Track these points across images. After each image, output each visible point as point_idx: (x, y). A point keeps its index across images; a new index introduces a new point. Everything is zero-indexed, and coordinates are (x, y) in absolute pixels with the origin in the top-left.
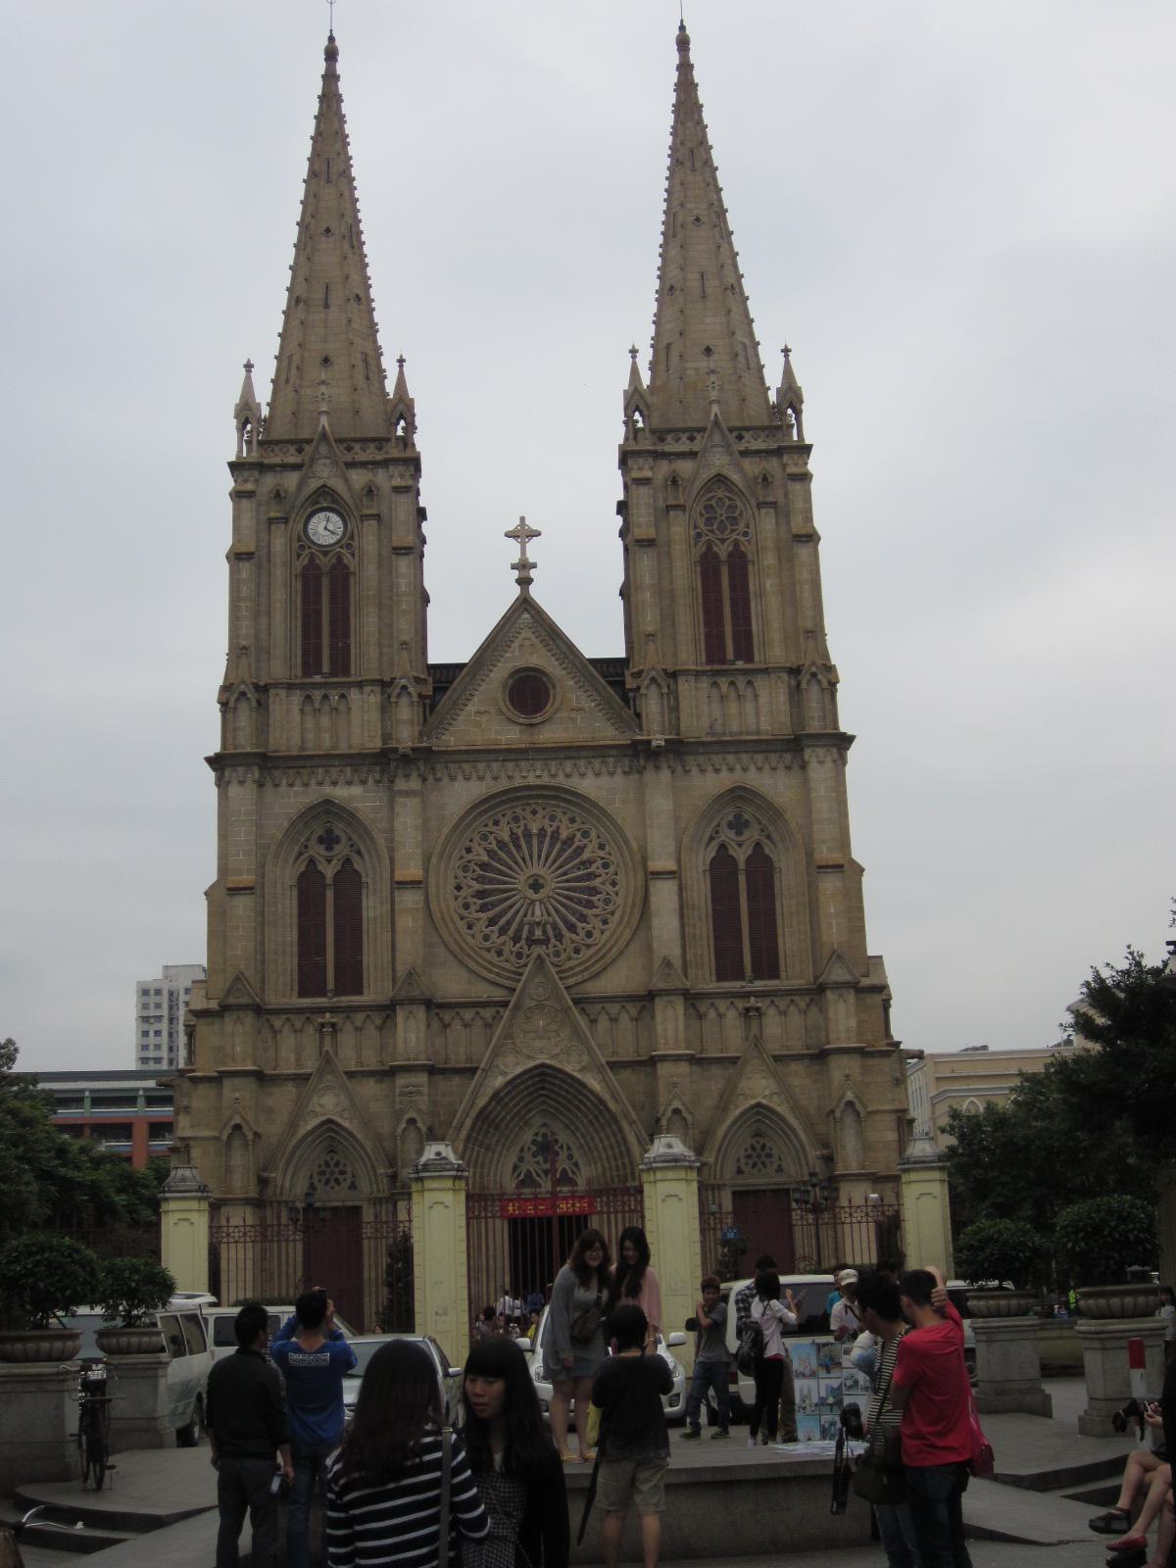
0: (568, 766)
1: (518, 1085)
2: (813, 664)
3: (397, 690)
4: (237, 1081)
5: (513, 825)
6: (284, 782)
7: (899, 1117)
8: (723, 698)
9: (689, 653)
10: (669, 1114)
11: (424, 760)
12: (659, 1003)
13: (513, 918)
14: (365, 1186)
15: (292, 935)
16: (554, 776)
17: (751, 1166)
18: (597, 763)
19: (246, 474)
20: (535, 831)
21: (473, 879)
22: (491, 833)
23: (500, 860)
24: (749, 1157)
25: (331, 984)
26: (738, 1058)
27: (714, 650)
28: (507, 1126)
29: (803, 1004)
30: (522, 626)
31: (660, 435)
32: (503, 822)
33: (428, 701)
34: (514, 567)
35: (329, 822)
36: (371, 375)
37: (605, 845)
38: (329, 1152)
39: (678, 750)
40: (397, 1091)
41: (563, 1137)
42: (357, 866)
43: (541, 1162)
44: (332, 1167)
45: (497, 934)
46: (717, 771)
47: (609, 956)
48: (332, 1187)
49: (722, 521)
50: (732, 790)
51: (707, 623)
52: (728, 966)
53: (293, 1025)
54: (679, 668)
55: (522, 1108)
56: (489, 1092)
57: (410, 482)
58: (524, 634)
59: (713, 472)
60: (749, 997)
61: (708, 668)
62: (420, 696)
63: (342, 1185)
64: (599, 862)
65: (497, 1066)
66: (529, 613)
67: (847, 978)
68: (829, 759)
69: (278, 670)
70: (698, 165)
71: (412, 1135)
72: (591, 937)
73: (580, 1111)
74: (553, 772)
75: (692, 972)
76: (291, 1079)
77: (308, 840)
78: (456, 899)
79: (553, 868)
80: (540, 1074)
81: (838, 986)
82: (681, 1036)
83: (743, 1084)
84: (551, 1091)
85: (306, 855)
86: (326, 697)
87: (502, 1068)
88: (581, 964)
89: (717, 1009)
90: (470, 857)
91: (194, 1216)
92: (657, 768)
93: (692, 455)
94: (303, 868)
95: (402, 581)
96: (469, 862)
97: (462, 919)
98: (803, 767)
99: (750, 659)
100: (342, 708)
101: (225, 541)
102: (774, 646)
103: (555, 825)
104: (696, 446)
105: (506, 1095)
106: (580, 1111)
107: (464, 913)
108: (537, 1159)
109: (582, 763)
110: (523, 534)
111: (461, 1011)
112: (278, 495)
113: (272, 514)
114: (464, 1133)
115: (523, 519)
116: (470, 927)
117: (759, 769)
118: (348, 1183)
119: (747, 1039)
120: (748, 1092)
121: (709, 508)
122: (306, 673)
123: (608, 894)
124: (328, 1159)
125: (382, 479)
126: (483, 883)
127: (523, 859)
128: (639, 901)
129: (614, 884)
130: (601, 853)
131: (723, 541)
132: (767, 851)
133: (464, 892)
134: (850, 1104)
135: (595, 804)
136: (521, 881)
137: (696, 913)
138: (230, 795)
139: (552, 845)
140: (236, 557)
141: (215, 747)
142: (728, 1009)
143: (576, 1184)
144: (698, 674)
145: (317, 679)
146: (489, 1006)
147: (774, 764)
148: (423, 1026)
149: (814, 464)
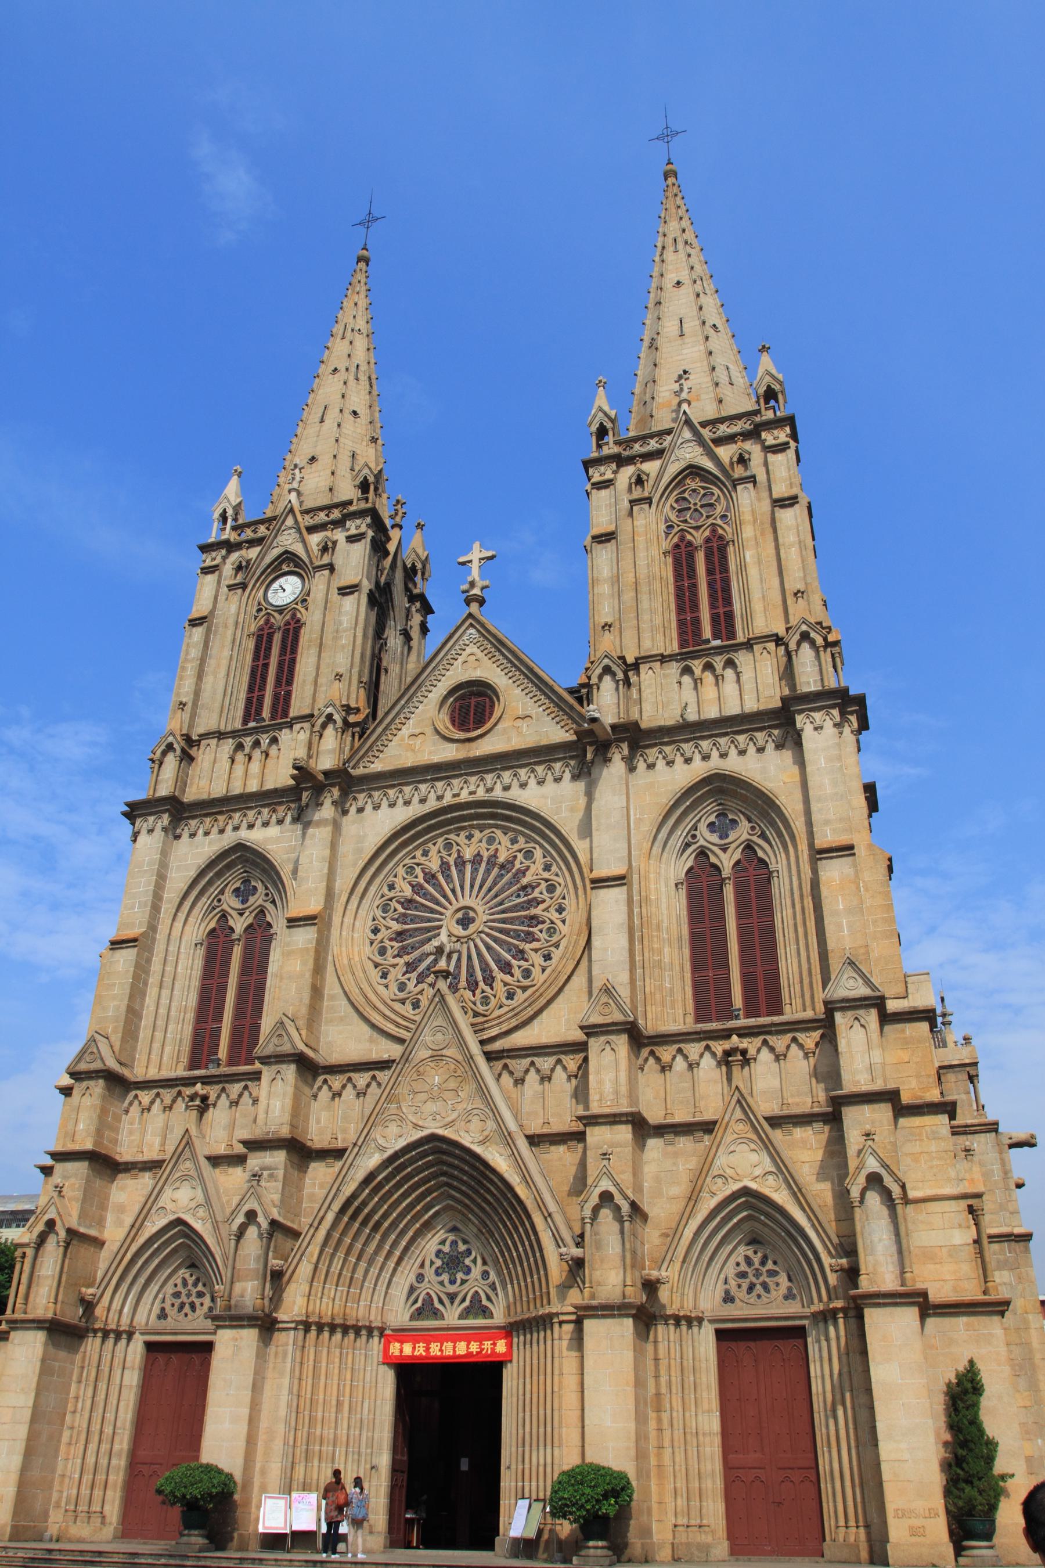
0: (507, 776)
2: (804, 622)
3: (322, 719)
5: (444, 853)
6: (201, 832)
7: (970, 1207)
8: (697, 682)
16: (489, 790)
17: (745, 1286)
18: (540, 769)
21: (393, 920)
22: (418, 865)
23: (426, 895)
24: (743, 1275)
25: (223, 1052)
26: (715, 1123)
28: (394, 1224)
29: (812, 1045)
30: (467, 642)
31: (628, 442)
32: (433, 850)
33: (357, 729)
35: (245, 872)
37: (550, 866)
43: (446, 1282)
44: (190, 1287)
46: (688, 761)
48: (186, 1315)
49: (696, 510)
51: (680, 609)
56: (360, 1175)
57: (363, 528)
58: (469, 650)
60: (729, 1037)
62: (345, 722)
64: (544, 885)
65: (375, 1140)
66: (475, 628)
68: (828, 724)
72: (528, 977)
76: (150, 1169)
77: (222, 892)
78: (372, 943)
83: (722, 1160)
84: (452, 1177)
86: (257, 744)
92: (607, 760)
94: (212, 925)
97: (376, 967)
100: (273, 751)
103: (493, 848)
105: (387, 1179)
107: (378, 959)
108: (440, 1279)
109: (523, 772)
111: (355, 1076)
113: (232, 582)
116: (384, 976)
117: (742, 753)
120: (729, 1172)
123: (552, 922)
125: (339, 535)
126: (405, 923)
127: (453, 891)
129: (560, 910)
130: (546, 875)
131: (697, 528)
132: (760, 854)
133: (380, 936)
134: (874, 1180)
139: (488, 872)
142: (701, 1056)
143: (491, 1316)
144: (663, 659)
147: (761, 743)
148: (290, 1090)
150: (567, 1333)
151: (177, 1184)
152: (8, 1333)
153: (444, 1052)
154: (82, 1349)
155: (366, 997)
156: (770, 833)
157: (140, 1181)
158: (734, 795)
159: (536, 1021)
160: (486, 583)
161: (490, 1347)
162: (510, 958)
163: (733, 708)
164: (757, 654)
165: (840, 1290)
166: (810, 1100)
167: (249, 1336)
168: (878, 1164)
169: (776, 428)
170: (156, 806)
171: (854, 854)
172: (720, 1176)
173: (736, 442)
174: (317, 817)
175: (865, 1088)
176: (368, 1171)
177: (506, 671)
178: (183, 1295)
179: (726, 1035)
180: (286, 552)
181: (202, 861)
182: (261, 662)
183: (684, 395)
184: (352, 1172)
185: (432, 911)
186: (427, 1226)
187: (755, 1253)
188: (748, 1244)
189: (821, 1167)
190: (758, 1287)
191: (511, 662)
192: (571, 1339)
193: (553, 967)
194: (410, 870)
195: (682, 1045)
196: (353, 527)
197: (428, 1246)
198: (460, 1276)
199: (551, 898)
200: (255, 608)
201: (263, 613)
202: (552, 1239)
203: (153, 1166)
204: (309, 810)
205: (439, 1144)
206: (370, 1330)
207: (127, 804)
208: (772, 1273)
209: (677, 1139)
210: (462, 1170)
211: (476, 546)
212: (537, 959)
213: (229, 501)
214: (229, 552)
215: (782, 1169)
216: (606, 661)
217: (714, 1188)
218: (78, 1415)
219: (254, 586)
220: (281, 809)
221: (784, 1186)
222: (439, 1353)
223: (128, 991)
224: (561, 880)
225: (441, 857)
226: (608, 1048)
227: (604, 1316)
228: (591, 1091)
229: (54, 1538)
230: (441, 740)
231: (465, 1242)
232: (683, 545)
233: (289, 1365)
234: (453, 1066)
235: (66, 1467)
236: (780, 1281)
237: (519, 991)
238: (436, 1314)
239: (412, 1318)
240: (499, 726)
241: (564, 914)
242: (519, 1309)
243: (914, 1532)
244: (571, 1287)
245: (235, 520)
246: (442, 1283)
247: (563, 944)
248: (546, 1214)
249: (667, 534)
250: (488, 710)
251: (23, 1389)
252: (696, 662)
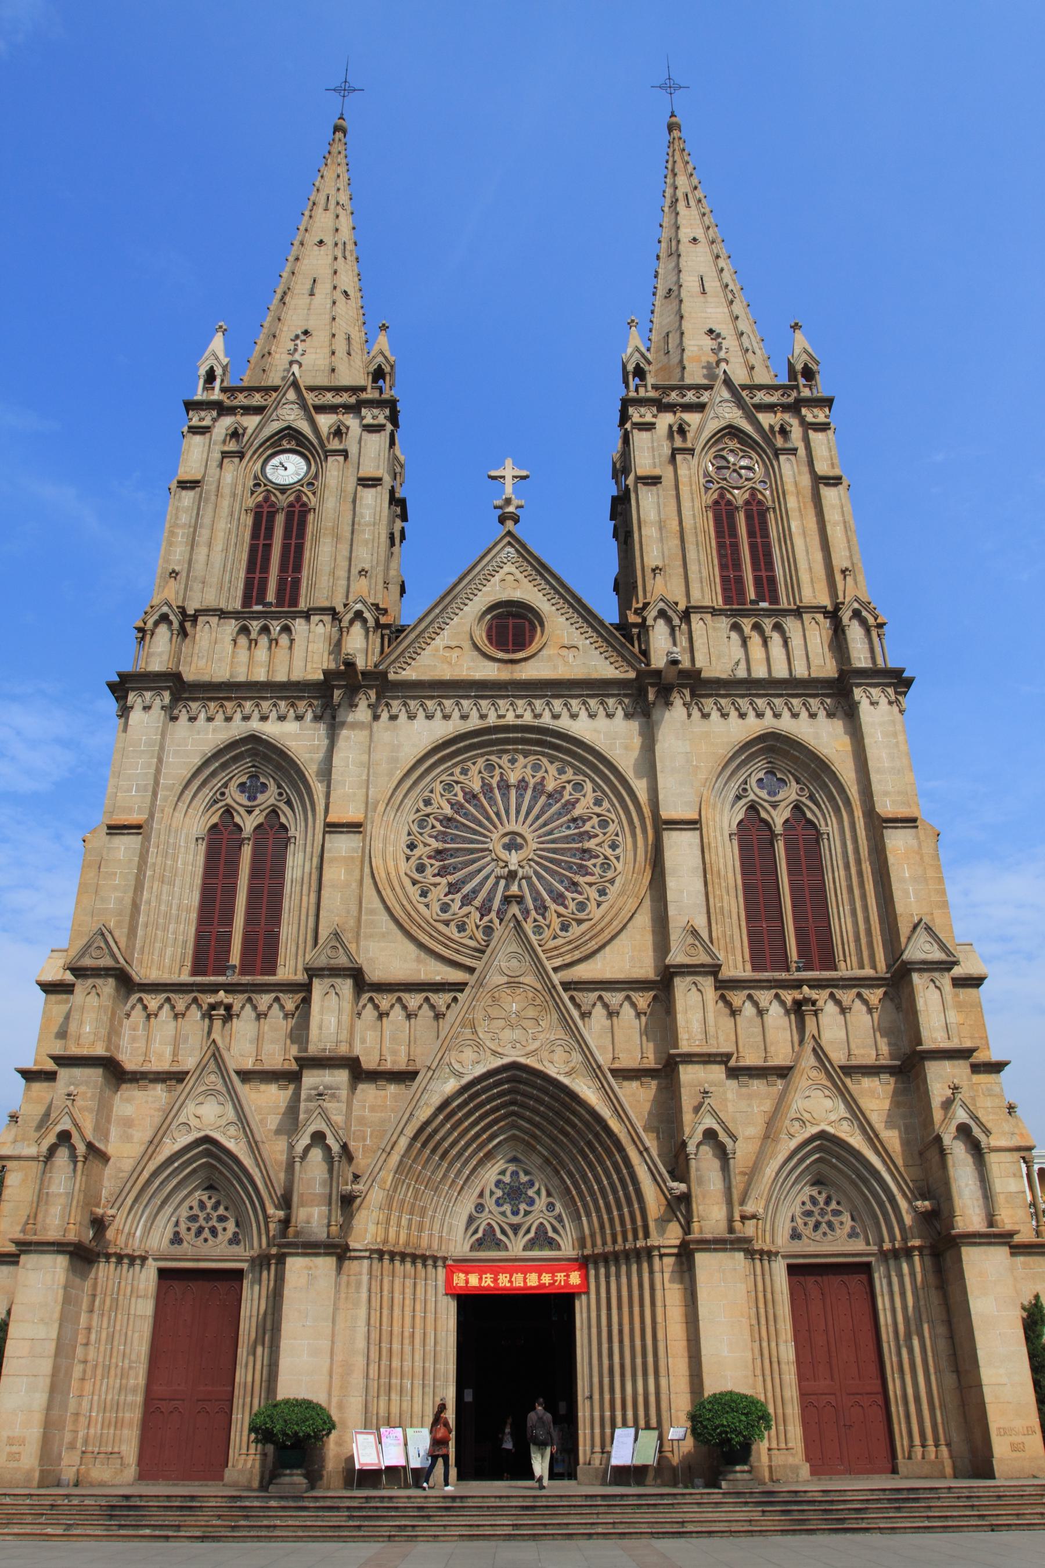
0: (557, 704)
1: (477, 1094)
2: (857, 600)
3: (350, 615)
4: (78, 1072)
5: (486, 775)
6: (202, 716)
10: (698, 1136)
12: (680, 984)
13: (482, 884)
15: (193, 899)
16: (537, 716)
17: (811, 1224)
18: (593, 702)
19: (203, 414)
21: (431, 836)
22: (457, 783)
23: (466, 815)
24: (808, 1214)
25: (235, 958)
26: (790, 1068)
27: (732, 587)
28: (460, 1154)
29: (876, 1002)
30: (505, 560)
32: (474, 770)
33: (387, 632)
35: (253, 766)
36: (352, 352)
37: (602, 800)
38: (206, 1189)
40: (303, 1096)
42: (286, 817)
43: (509, 1213)
44: (209, 1210)
45: (460, 904)
47: (606, 932)
48: (206, 1240)
51: (723, 567)
53: (173, 1007)
54: (693, 603)
55: (484, 1130)
56: (436, 1100)
57: (381, 420)
58: (507, 568)
59: (723, 423)
60: (800, 987)
61: (728, 607)
62: (377, 621)
63: (220, 1236)
64: (595, 820)
65: (450, 1065)
66: (513, 546)
67: (938, 955)
68: (883, 701)
69: (211, 599)
70: (692, 203)
71: (316, 1155)
72: (584, 910)
73: (566, 1134)
74: (538, 711)
76: (163, 1081)
77: (226, 785)
78: (408, 859)
79: (535, 826)
80: (508, 1080)
85: (223, 803)
86: (265, 630)
87: (457, 1066)
88: (570, 942)
89: (756, 1004)
90: (429, 810)
92: (668, 704)
93: (700, 407)
94: (215, 819)
96: (428, 815)
97: (414, 884)
99: (775, 599)
100: (284, 640)
103: (539, 775)
104: (705, 397)
105: (460, 1107)
106: (566, 1134)
107: (417, 876)
108: (502, 1209)
109: (574, 702)
111: (406, 996)
112: (235, 435)
113: (226, 449)
114: (395, 1158)
116: (424, 894)
117: (795, 715)
118: (229, 1234)
119: (801, 1041)
120: (806, 1116)
122: (247, 600)
123: (606, 858)
124: (205, 1198)
125: (351, 421)
126: (445, 842)
127: (497, 814)
129: (614, 846)
130: (597, 810)
132: (809, 815)
133: (417, 852)
136: (496, 842)
137: (723, 884)
138: (130, 722)
139: (535, 799)
143: (559, 1248)
145: (258, 608)
146: (444, 991)
147: (814, 709)
149: (835, 416)
150: (668, 1266)
151: (201, 1099)
152: (18, 1256)
153: (521, 979)
154: (92, 1275)
155: (409, 915)
157: (151, 1093)
158: (785, 754)
159: (598, 956)
160: (522, 502)
161: (563, 1278)
162: (563, 890)
163: (781, 671)
164: (806, 623)
165: (915, 1230)
166: (874, 1053)
167: (326, 1264)
168: (967, 1116)
169: (816, 407)
170: (154, 681)
171: (917, 827)
172: (797, 1119)
173: (775, 413)
174: (351, 718)
175: (945, 1045)
176: (446, 1096)
177: (549, 597)
178: (201, 1219)
179: (797, 985)
180: (289, 428)
181: (208, 749)
182: (262, 542)
183: (722, 354)
184: (426, 1096)
185: (475, 832)
186: (489, 1156)
187: (820, 1193)
188: (813, 1185)
189: (889, 1116)
190: (824, 1225)
191: (553, 588)
192: (672, 1272)
193: (611, 902)
194: (448, 787)
195: (752, 992)
196: (369, 416)
197: (487, 1176)
198: (523, 1207)
199: (605, 834)
200: (252, 483)
201: (262, 489)
202: (648, 1173)
203: (176, 1077)
204: (341, 709)
205: (518, 1073)
206: (435, 1259)
207: (120, 675)
208: (836, 1213)
209: (751, 1081)
210: (541, 1102)
211: (509, 462)
212: (593, 893)
213: (217, 358)
214: (219, 415)
215: (857, 1114)
216: (662, 605)
217: (792, 1131)
218: (91, 1348)
219: (251, 457)
220: (302, 705)
221: (858, 1131)
222: (508, 1285)
223: (133, 883)
224: (614, 817)
225: (482, 778)
226: (694, 989)
227: (716, 1250)
228: (680, 1030)
229: (71, 1484)
230: (480, 657)
231: (527, 1173)
232: (723, 503)
233: (364, 1295)
234: (531, 995)
235: (80, 1404)
236: (844, 1220)
237: (573, 923)
238: (499, 1245)
239: (472, 1248)
240: (544, 652)
241: (618, 851)
242: (599, 1241)
243: (1015, 1447)
244: (670, 1221)
245: (222, 381)
246: (503, 1214)
247: (618, 880)
248: (642, 1149)
249: (707, 489)
250: (527, 634)
251: (42, 1320)
252: (745, 620)
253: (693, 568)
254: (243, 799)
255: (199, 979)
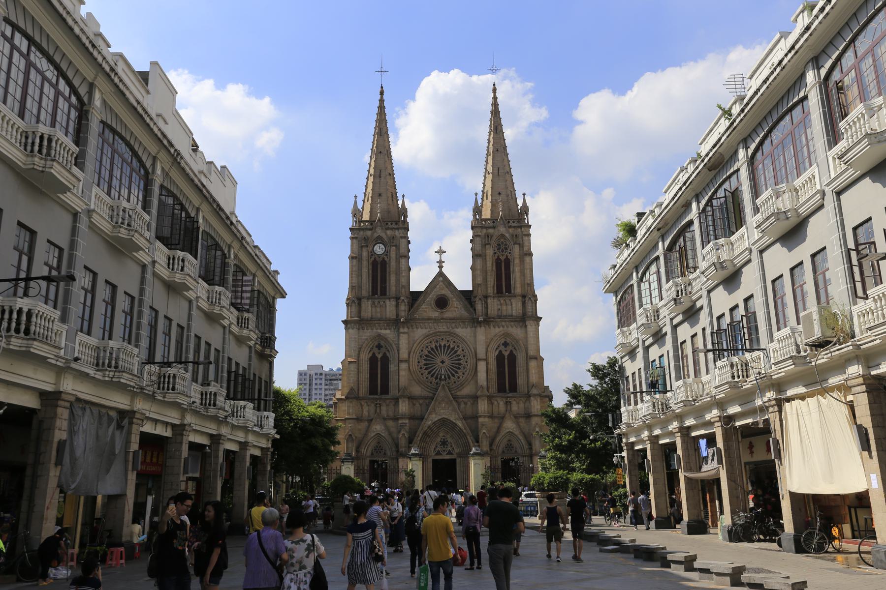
0: (453, 325)
4: (350, 421)
9: (491, 290)
11: (410, 322)
13: (435, 372)
14: (388, 453)
15: (368, 376)
20: (442, 345)
23: (432, 354)
29: (524, 401)
34: (437, 262)
39: (488, 321)
41: (449, 440)
42: (388, 354)
50: (504, 334)
52: (501, 389)
64: (462, 355)
75: (490, 390)
81: (535, 395)
82: (486, 410)
83: (505, 425)
86: (379, 302)
90: (422, 353)
91: (350, 466)
92: (481, 327)
93: (494, 228)
95: (403, 267)
98: (526, 326)
99: (510, 292)
100: (384, 306)
101: (348, 252)
102: (518, 290)
103: (449, 343)
110: (441, 252)
114: (419, 438)
115: (440, 247)
116: (422, 374)
117: (512, 327)
121: (499, 245)
128: (474, 368)
129: (467, 362)
130: (463, 352)
131: (503, 255)
132: (514, 352)
133: (420, 364)
135: (460, 337)
136: (438, 360)
139: (448, 350)
140: (352, 258)
141: (345, 318)
148: (407, 405)
149: (531, 231)
156: (517, 348)
212: (461, 374)
253: (489, 283)
254: (377, 349)
255: (372, 397)
